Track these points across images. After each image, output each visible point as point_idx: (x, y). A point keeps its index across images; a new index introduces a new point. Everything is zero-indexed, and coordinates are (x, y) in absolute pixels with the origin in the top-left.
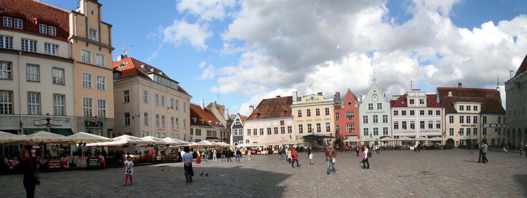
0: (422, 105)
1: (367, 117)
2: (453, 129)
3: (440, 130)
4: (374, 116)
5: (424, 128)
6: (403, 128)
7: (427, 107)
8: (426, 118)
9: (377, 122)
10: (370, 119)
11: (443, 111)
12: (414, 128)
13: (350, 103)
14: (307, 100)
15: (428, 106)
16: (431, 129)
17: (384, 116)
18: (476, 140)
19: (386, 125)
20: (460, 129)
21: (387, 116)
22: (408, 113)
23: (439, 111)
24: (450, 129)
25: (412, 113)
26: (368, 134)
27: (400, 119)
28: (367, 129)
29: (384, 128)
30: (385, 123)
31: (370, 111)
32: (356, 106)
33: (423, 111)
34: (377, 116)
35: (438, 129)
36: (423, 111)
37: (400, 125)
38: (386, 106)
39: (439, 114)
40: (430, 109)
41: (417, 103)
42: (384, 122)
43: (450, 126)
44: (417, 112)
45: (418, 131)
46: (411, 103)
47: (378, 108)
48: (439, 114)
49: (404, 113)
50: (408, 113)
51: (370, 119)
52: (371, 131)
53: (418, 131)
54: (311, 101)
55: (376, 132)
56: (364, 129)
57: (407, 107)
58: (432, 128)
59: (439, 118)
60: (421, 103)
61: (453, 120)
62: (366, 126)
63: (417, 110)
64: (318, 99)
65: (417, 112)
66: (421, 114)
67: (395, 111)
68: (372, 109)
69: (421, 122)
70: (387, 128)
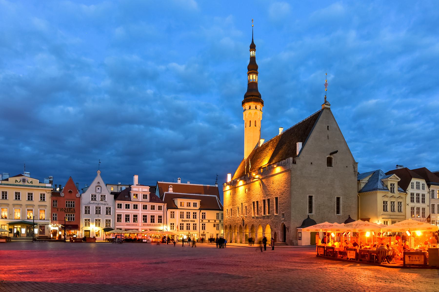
0: (145, 200)
1: (89, 207)
2: (173, 224)
4: (96, 208)
5: (146, 222)
7: (150, 202)
8: (149, 212)
9: (100, 213)
11: (164, 206)
15: (151, 201)
17: (107, 208)
20: (181, 224)
22: (131, 207)
23: (161, 207)
25: (136, 207)
27: (123, 212)
31: (92, 202)
36: (146, 206)
37: (123, 218)
39: (161, 209)
41: (140, 197)
44: (140, 206)
47: (102, 200)
48: (161, 209)
49: (128, 206)
50: (131, 207)
57: (131, 200)
58: (154, 222)
59: (161, 213)
60: (144, 198)
61: (174, 215)
65: (140, 206)
66: (144, 208)
67: (118, 204)
68: (95, 200)
69: (144, 216)
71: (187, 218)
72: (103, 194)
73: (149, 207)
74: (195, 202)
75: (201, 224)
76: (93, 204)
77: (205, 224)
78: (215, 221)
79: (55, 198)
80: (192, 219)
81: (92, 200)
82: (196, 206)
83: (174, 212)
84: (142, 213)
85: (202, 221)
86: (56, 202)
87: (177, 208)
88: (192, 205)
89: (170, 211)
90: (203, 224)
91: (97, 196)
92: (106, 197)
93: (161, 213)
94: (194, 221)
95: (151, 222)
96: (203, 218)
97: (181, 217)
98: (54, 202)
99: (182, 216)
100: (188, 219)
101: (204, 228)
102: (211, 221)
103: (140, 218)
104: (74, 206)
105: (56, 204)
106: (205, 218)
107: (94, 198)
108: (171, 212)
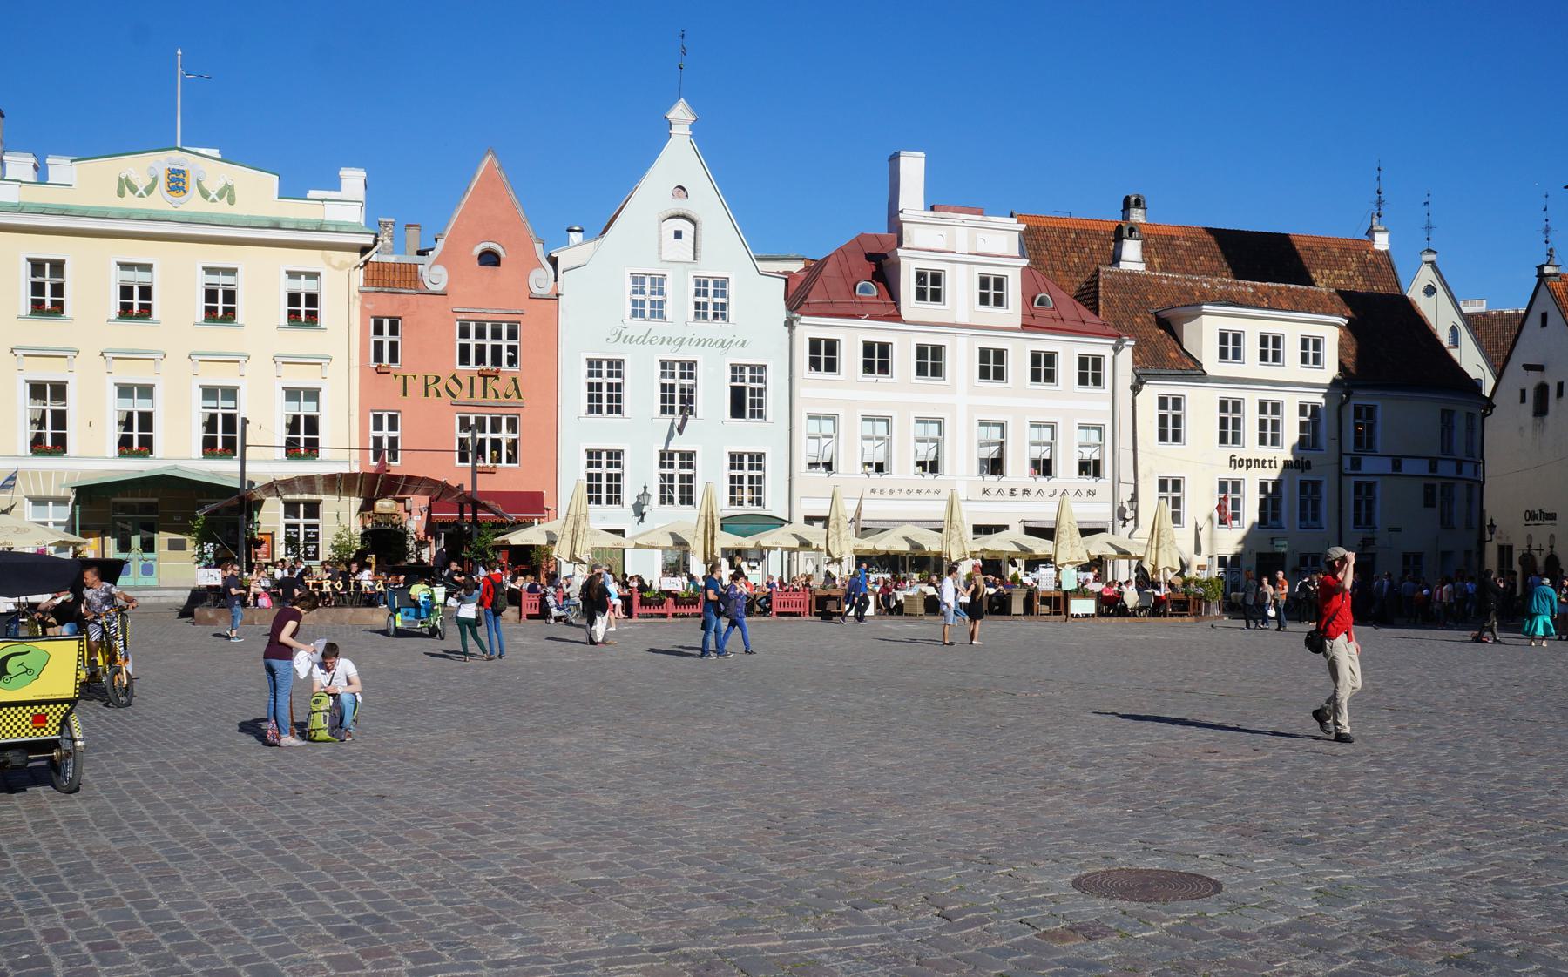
0: (991, 314)
1: (616, 366)
3: (1104, 484)
7: (1026, 327)
10: (642, 389)
11: (1121, 363)
13: (490, 259)
14: (125, 186)
19: (748, 435)
20: (1223, 486)
21: (758, 371)
22: (903, 359)
25: (930, 361)
26: (615, 497)
28: (615, 457)
29: (736, 459)
30: (747, 424)
31: (639, 326)
32: (540, 281)
33: (1000, 355)
34: (689, 368)
36: (1000, 355)
38: (758, 295)
39: (1097, 381)
40: (1045, 343)
42: (737, 410)
43: (1159, 460)
44: (961, 357)
46: (921, 295)
48: (1097, 381)
49: (877, 359)
50: (903, 359)
51: (642, 389)
52: (640, 474)
54: (160, 201)
55: (676, 488)
56: (593, 456)
57: (896, 317)
59: (1094, 404)
60: (984, 300)
62: (605, 432)
64: (227, 192)
65: (961, 357)
67: (815, 345)
68: (658, 311)
70: (757, 459)
71: (1262, 441)
72: (709, 269)
74: (1313, 331)
75: (1349, 484)
76: (643, 340)
77: (1370, 487)
78: (1433, 466)
79: (387, 306)
81: (637, 311)
82: (1317, 360)
83: (1177, 403)
85: (1356, 464)
86: (394, 331)
88: (1291, 350)
90: (1358, 486)
91: (669, 287)
92: (732, 288)
97: (1223, 439)
98: (378, 330)
99: (1229, 431)
102: (1408, 467)
104: (512, 361)
105: (393, 346)
106: (1370, 444)
107: (648, 299)
108: (1163, 402)
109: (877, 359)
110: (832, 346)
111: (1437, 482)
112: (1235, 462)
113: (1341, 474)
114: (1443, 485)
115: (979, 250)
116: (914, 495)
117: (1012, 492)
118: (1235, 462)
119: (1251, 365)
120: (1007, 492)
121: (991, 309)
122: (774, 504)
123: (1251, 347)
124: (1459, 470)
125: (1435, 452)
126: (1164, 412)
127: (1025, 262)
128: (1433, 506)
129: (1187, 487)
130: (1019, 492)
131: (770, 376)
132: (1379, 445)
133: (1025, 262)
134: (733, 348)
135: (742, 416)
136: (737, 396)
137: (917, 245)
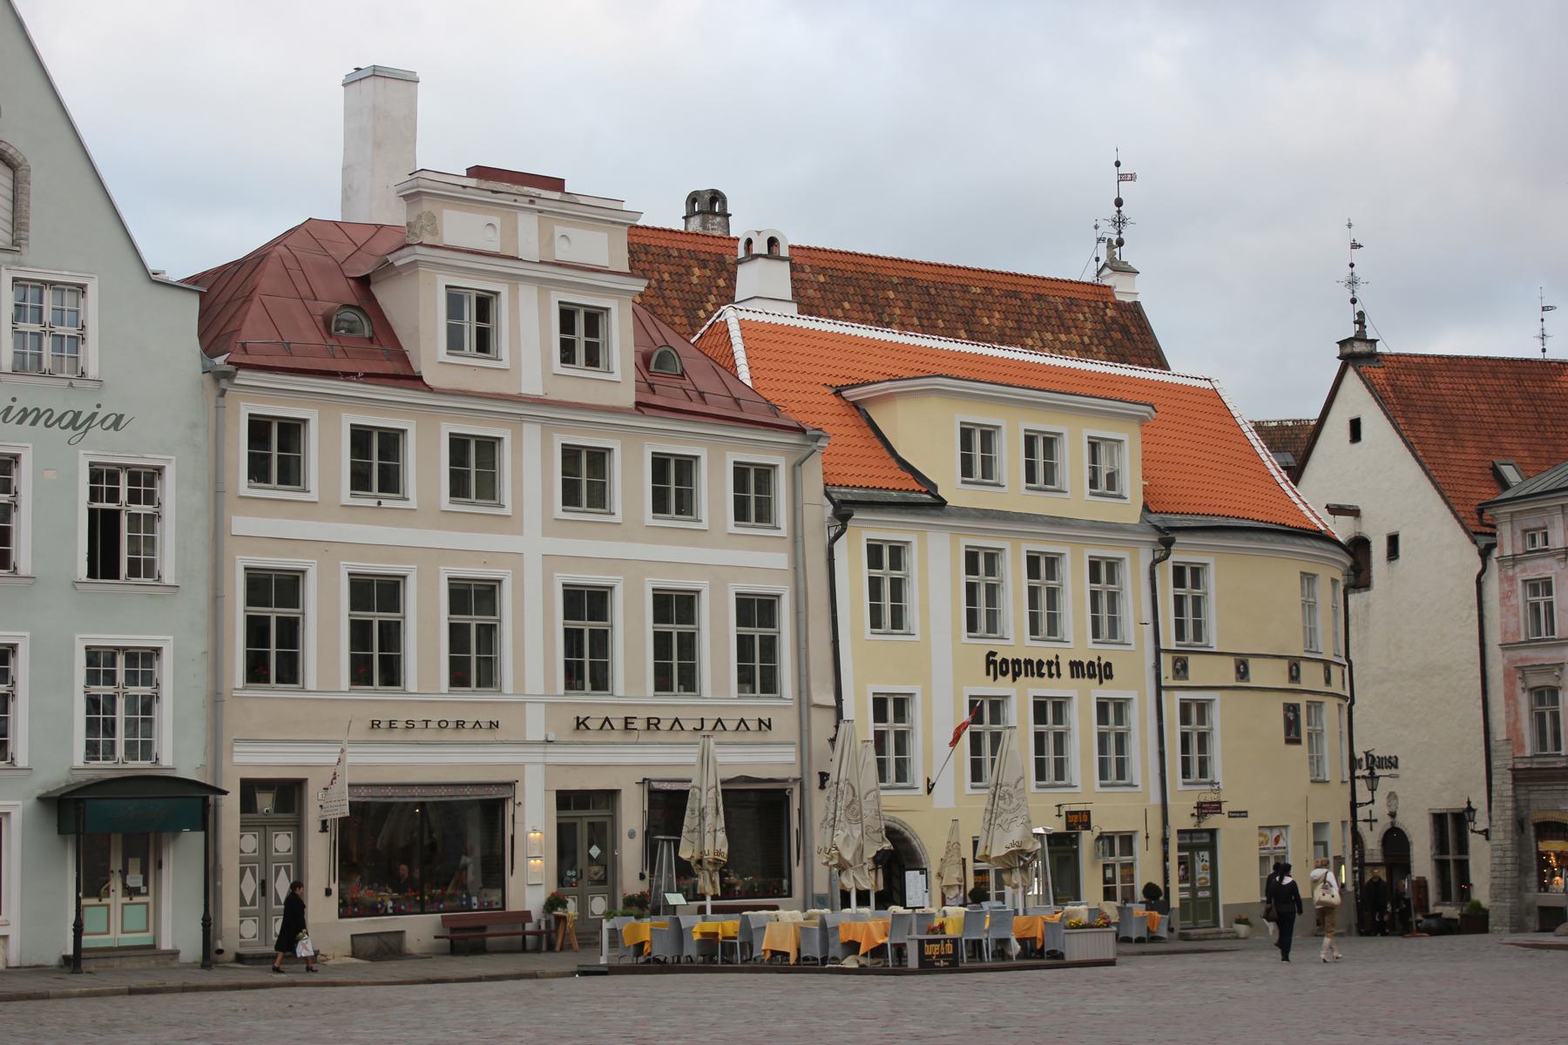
0: (579, 384)
2: (901, 703)
5: (601, 682)
6: (360, 675)
8: (633, 553)
12: (488, 678)
16: (675, 703)
18: (1127, 840)
19: (122, 616)
21: (145, 481)
22: (425, 464)
23: (765, 474)
24: (880, 704)
25: (473, 468)
27: (323, 532)
29: (99, 662)
30: (122, 588)
35: (757, 705)
36: (599, 458)
40: (678, 440)
42: (103, 562)
44: (530, 467)
45: (535, 725)
49: (376, 462)
50: (425, 464)
53: (535, 725)
58: (689, 682)
59: (758, 561)
60: (567, 354)
63: (532, 434)
65: (530, 467)
66: (571, 496)
67: (259, 429)
70: (143, 661)
73: (630, 480)
77: (1203, 706)
80: (1087, 650)
83: (897, 552)
84: (551, 561)
85: (1181, 669)
87: (926, 502)
88: (1073, 462)
89: (866, 529)
90: (1185, 707)
93: (758, 561)
94: (1104, 672)
95: (663, 683)
96: (1180, 634)
97: (972, 626)
99: (980, 611)
100: (1041, 650)
101: (1196, 754)
102: (1260, 674)
103: (531, 638)
108: (874, 552)
109: (376, 462)
110: (292, 431)
111: (1302, 700)
112: (997, 666)
113: (1159, 688)
114: (1310, 704)
115: (560, 256)
116: (449, 735)
117: (627, 721)
118: (997, 666)
119: (1010, 489)
120: (618, 724)
121: (579, 370)
122: (176, 751)
123: (1010, 457)
124: (1328, 681)
125: (1298, 651)
126: (876, 573)
127: (639, 285)
128: (1298, 742)
129: (916, 711)
130: (640, 724)
131: (168, 490)
132: (1214, 637)
133: (639, 285)
134: (96, 432)
135: (115, 575)
136: (103, 529)
137: (448, 240)
